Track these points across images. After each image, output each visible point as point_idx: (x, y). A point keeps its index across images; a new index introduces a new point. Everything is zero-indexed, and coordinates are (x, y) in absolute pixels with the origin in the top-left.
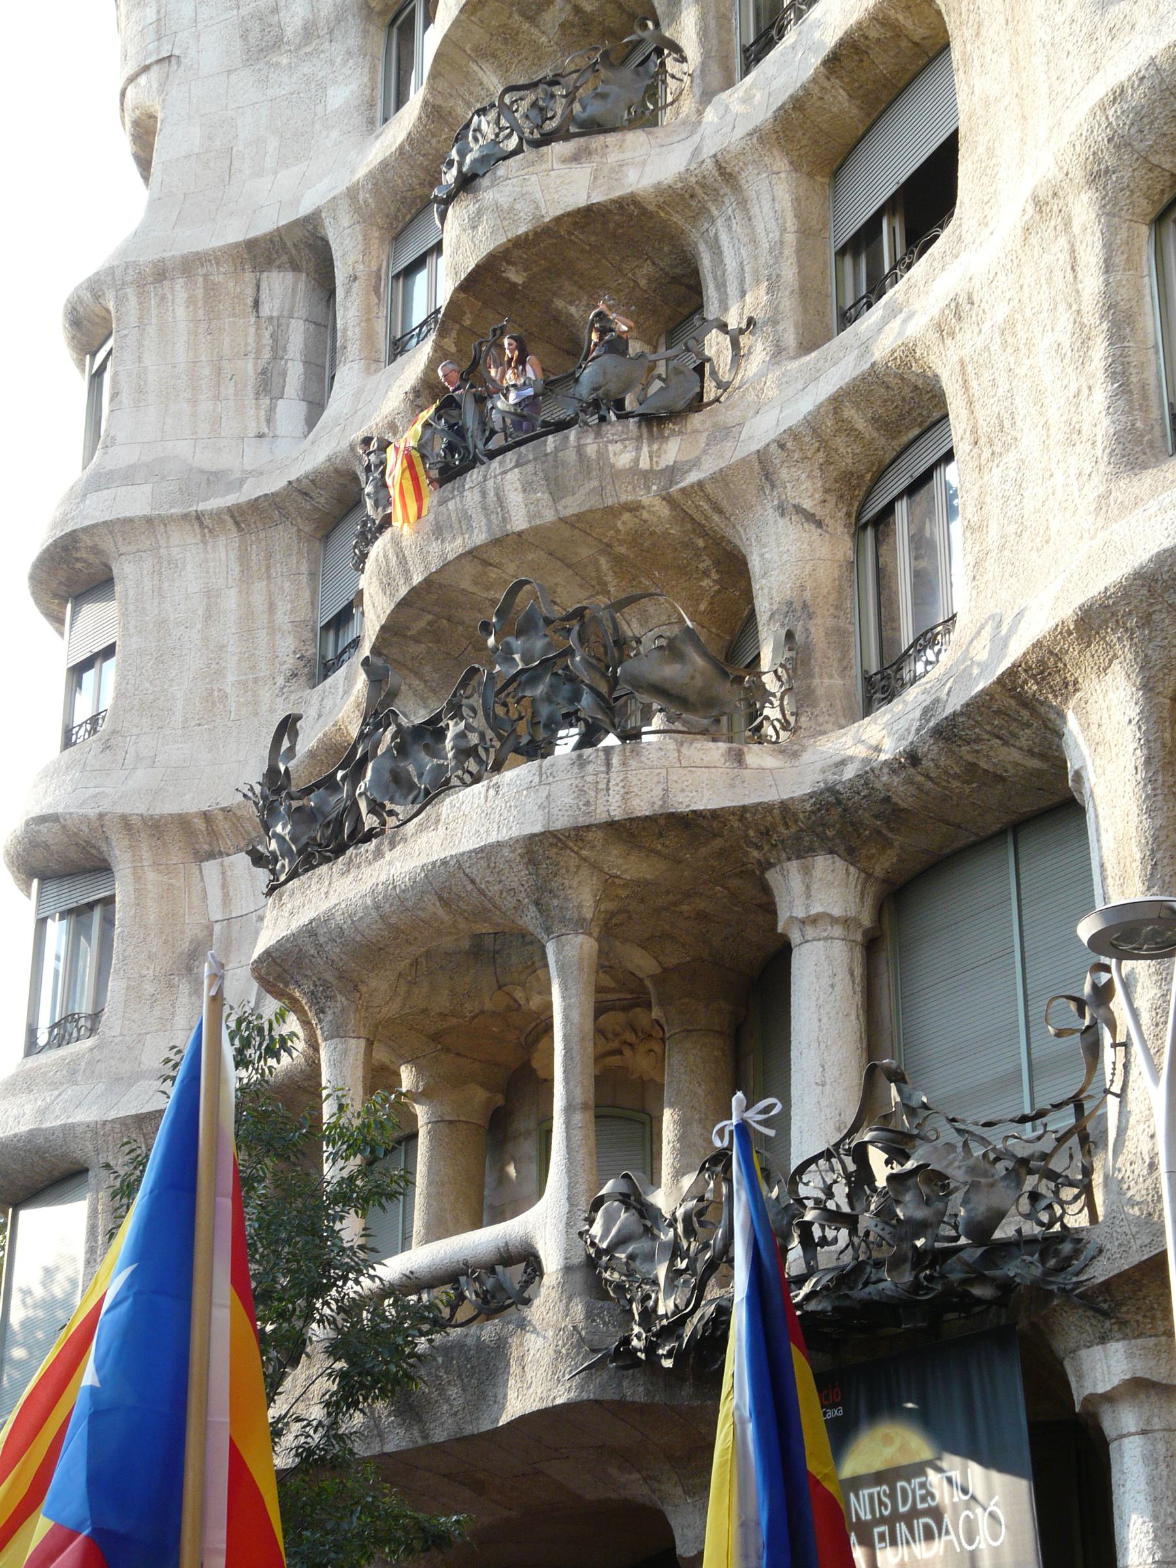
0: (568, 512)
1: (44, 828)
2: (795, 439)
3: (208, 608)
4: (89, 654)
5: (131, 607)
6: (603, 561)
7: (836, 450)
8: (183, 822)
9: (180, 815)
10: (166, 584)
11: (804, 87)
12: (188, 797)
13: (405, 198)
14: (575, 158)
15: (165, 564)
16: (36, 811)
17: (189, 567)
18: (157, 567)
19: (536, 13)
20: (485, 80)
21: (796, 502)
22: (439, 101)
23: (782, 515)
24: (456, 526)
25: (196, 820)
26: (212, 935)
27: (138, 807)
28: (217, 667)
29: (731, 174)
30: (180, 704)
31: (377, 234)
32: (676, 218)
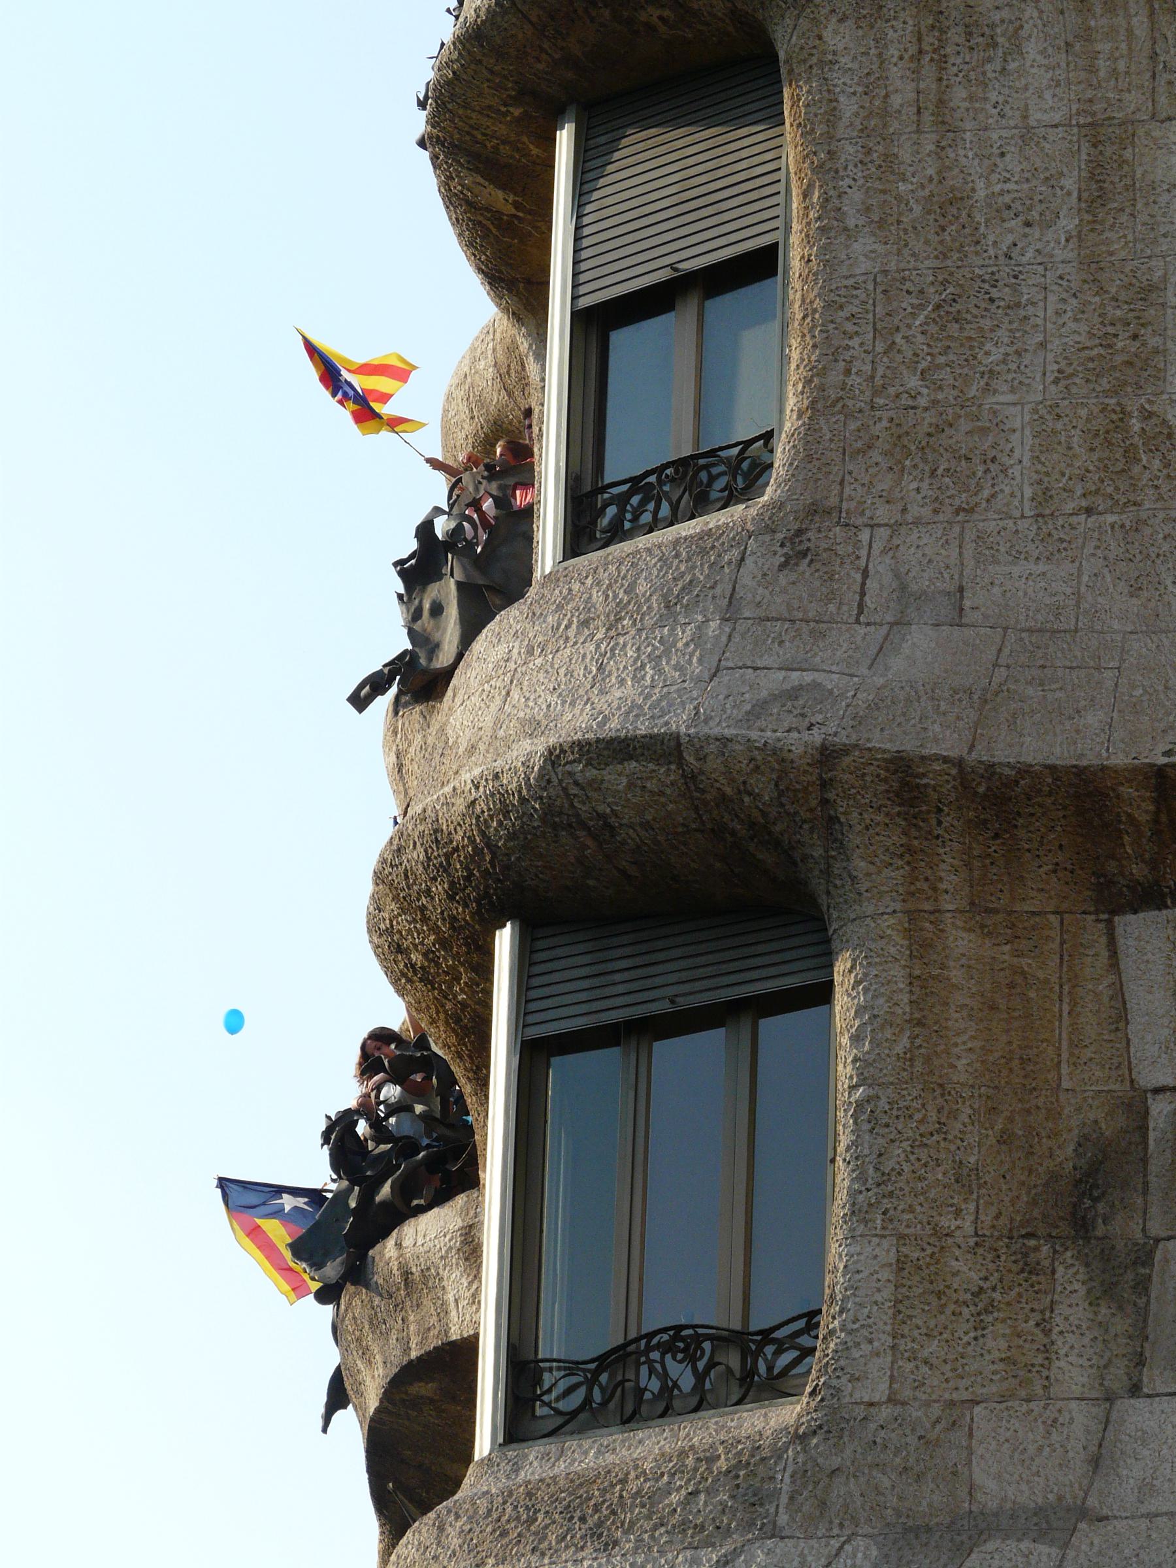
1: (616, 777)
3: (1096, 174)
4: (664, 275)
5: (849, 151)
8: (1084, 795)
9: (1080, 772)
10: (959, 95)
12: (1093, 719)
15: (955, 35)
16: (577, 723)
17: (1031, 49)
18: (929, 40)
25: (1127, 791)
26: (1143, 1129)
27: (942, 738)
28: (1134, 347)
30: (1022, 445)
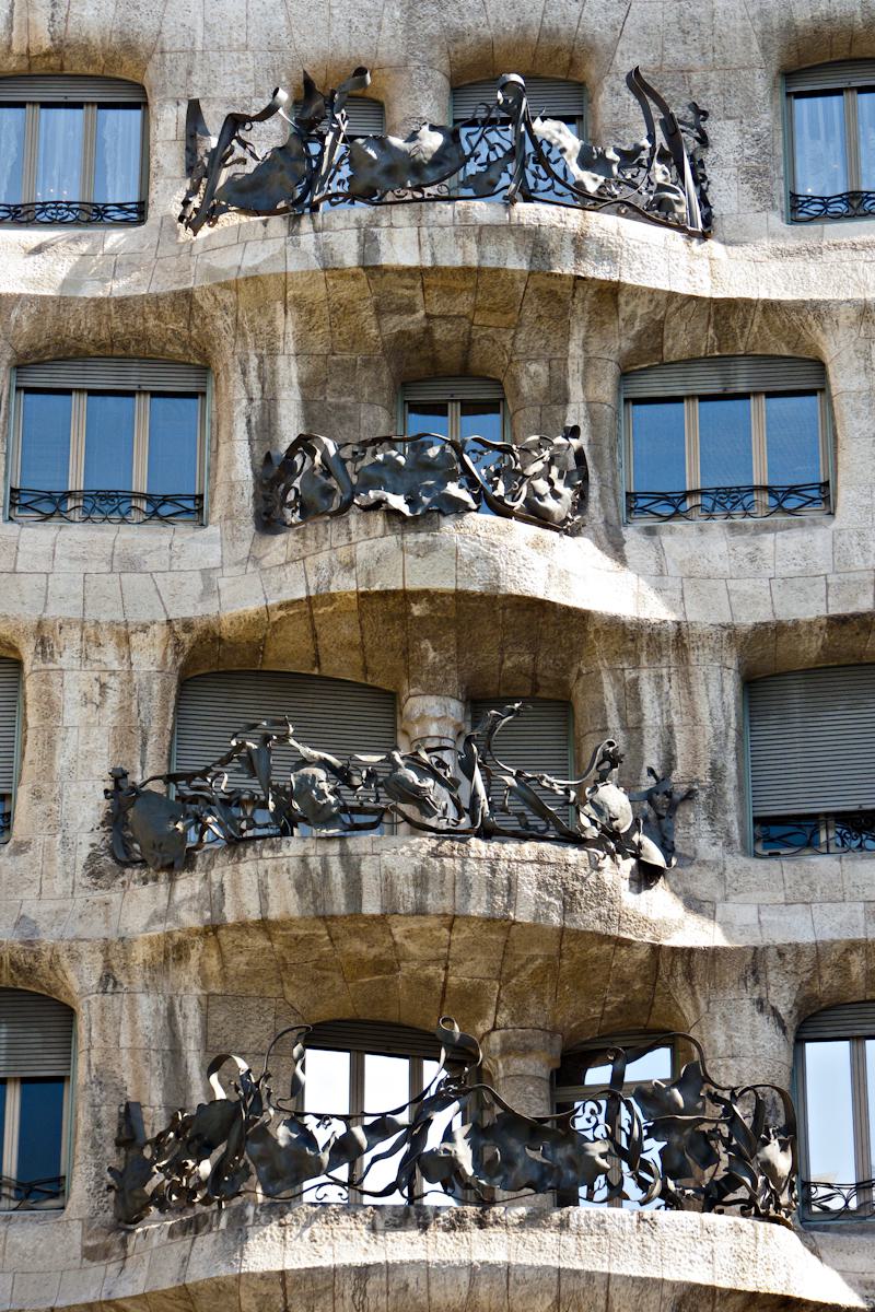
0: (574, 926)
2: (797, 955)
6: (540, 961)
7: (821, 977)
11: (796, 623)
13: (64, 342)
14: (537, 544)
19: (391, 312)
20: (279, 322)
21: (774, 1004)
22: (207, 305)
23: (761, 1011)
24: (449, 885)
29: (685, 645)
31: (9, 357)
32: (600, 645)
